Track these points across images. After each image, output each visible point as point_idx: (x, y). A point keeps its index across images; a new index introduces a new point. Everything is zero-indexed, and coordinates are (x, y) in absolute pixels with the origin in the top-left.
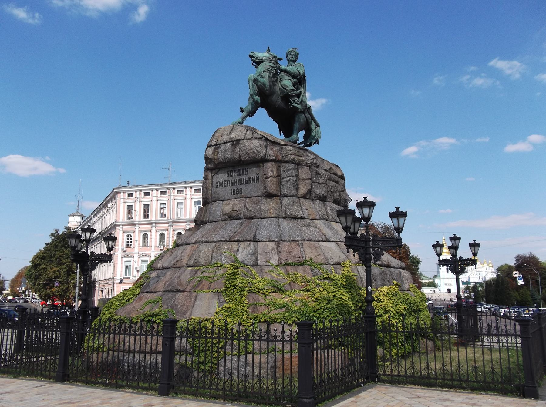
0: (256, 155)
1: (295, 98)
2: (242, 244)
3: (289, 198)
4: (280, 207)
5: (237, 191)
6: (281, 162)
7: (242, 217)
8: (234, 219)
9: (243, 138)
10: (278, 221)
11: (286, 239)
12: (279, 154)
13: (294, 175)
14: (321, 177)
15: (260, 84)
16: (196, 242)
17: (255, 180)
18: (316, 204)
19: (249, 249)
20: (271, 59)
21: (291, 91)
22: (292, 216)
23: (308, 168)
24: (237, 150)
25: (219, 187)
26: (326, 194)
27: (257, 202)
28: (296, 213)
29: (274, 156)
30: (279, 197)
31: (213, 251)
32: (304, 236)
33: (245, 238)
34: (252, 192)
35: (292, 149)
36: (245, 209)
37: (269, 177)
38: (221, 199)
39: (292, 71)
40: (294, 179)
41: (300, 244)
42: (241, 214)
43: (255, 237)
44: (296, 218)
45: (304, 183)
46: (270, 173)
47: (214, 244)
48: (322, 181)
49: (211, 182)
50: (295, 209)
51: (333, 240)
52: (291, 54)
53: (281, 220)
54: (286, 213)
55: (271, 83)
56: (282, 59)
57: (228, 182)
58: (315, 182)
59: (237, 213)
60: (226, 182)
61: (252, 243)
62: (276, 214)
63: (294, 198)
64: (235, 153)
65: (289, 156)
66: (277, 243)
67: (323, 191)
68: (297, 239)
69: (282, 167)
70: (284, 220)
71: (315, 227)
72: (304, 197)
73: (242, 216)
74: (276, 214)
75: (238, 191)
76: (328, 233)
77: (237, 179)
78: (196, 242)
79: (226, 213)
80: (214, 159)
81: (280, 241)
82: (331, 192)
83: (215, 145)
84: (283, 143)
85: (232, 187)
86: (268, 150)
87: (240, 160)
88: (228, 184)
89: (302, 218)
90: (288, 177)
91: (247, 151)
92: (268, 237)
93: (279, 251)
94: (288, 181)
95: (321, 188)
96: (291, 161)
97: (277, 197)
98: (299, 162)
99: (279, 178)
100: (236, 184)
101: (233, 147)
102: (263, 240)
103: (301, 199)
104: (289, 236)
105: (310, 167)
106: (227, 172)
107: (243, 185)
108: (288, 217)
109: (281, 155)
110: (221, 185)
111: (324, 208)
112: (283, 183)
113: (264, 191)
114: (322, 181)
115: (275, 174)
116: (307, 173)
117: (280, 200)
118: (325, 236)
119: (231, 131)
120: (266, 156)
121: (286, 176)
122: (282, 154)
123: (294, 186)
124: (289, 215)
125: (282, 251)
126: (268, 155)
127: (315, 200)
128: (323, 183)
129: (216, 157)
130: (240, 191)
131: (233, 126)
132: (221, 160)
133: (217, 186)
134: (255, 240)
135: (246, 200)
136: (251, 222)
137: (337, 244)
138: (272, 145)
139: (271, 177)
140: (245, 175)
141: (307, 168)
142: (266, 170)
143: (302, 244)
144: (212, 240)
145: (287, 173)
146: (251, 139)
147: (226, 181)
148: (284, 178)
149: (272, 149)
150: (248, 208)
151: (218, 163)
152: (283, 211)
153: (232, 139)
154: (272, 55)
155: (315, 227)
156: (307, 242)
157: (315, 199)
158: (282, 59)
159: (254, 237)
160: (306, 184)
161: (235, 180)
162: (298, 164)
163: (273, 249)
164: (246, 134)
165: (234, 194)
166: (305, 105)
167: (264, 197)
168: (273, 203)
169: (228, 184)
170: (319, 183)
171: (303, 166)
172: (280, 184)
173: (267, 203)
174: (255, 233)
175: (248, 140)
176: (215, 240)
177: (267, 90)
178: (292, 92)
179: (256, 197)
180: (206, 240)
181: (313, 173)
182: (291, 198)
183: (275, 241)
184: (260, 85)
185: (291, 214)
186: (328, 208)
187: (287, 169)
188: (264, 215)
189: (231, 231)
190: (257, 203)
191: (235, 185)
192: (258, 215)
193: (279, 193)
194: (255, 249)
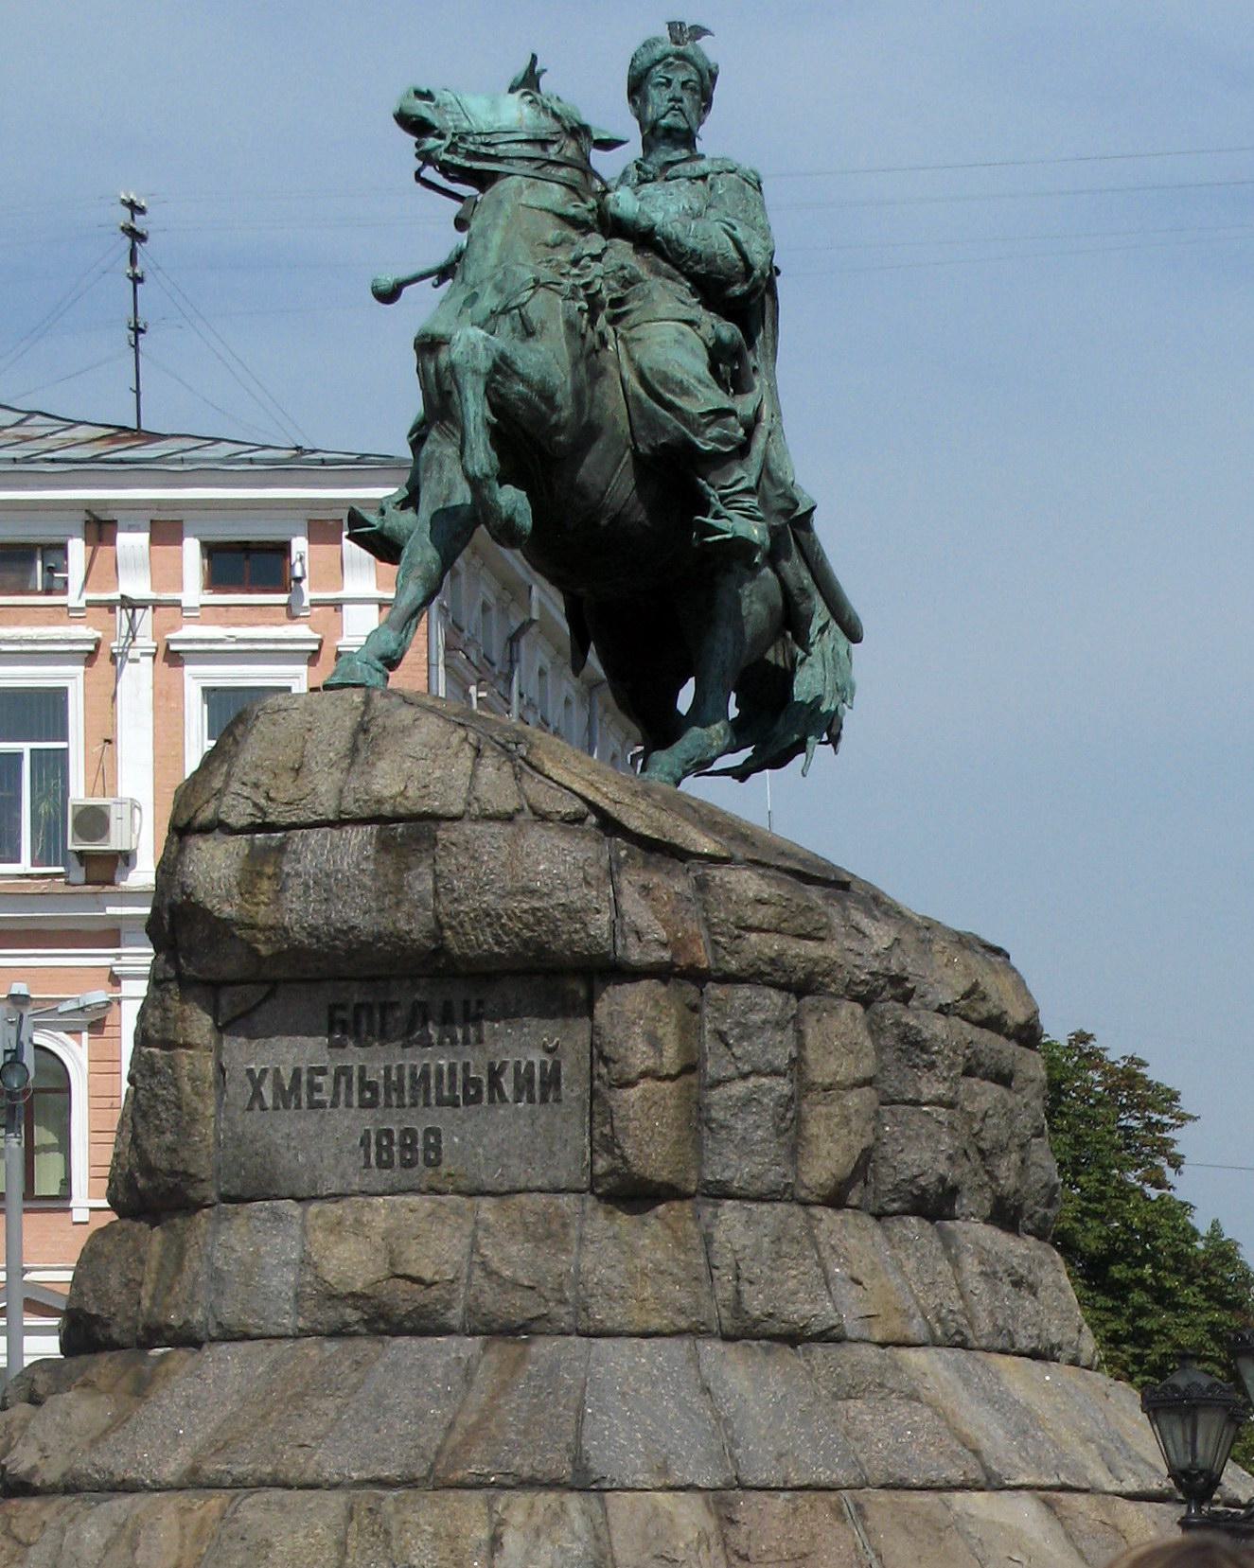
0: (555, 933)
1: (730, 472)
2: (518, 1508)
3: (753, 1206)
4: (704, 1271)
5: (404, 1146)
6: (697, 976)
7: (455, 1323)
8: (397, 1331)
9: (457, 808)
10: (695, 1359)
11: (762, 1477)
12: (693, 927)
13: (782, 1062)
14: (931, 1066)
15: (521, 388)
16: (194, 1482)
17: (531, 1081)
18: (904, 1239)
19: (562, 1533)
20: (553, 149)
21: (708, 425)
22: (776, 1327)
23: (859, 1009)
24: (421, 882)
25: (269, 1102)
26: (952, 1176)
27: (555, 1226)
28: (801, 1310)
29: (664, 945)
30: (688, 1203)
31: (342, 1545)
32: (863, 1457)
33: (524, 1465)
34: (515, 1161)
35: (767, 891)
36: (478, 1273)
37: (633, 1076)
38: (285, 1186)
39: (690, 243)
40: (783, 1086)
41: (848, 1507)
42: (448, 1306)
43: (578, 1458)
44: (794, 1338)
45: (835, 1109)
46: (640, 1057)
47: (336, 1500)
48: (932, 1088)
49: (211, 1065)
50: (792, 1284)
51: (1023, 1480)
52: (669, 83)
53: (711, 1348)
54: (737, 1307)
55: (582, 368)
56: (620, 143)
57: (337, 1082)
58: (894, 1102)
59: (423, 1296)
60: (320, 1079)
61: (574, 1502)
62: (681, 1311)
63: (779, 1206)
64: (406, 907)
65: (754, 937)
66: (719, 1502)
67: (942, 1157)
68: (824, 1476)
69: (707, 1010)
70: (732, 1351)
71: (913, 1397)
72: (836, 1199)
73: (455, 1316)
74: (681, 1311)
75: (411, 1148)
76: (989, 1437)
77: (400, 1068)
78: (194, 1482)
79: (343, 1290)
80: (252, 927)
81: (728, 1487)
82: (981, 1151)
83: (253, 828)
84: (706, 845)
85: (367, 1113)
86: (626, 904)
87: (441, 951)
88: (336, 1094)
89: (832, 1336)
90: (745, 1076)
91: (489, 898)
92: (659, 1461)
93: (736, 1552)
94: (747, 1102)
95: (930, 1136)
96: (761, 974)
97: (676, 1204)
98: (810, 976)
99: (692, 1079)
100: (401, 1098)
101: (388, 860)
102: (628, 1483)
103: (817, 1211)
104: (780, 1455)
105: (866, 1001)
106: (333, 1008)
107: (447, 1111)
108: (744, 1331)
109: (704, 932)
110: (286, 1096)
111: (943, 1266)
112: (717, 1114)
113: (602, 1164)
114: (932, 1088)
115: (670, 1058)
116: (852, 1049)
117: (697, 1218)
118: (976, 1453)
119: (355, 735)
120: (619, 942)
121: (731, 1071)
122: (710, 926)
123: (780, 1133)
124: (757, 1322)
125: (752, 1554)
126: (632, 939)
127: (895, 1213)
128: (939, 1102)
129: (263, 915)
130: (428, 1147)
131: (367, 702)
132: (299, 935)
133: (257, 1095)
134: (586, 1483)
135: (475, 1210)
136: (523, 1358)
137: (1049, 1505)
138: (646, 866)
139: (644, 1075)
140: (459, 1047)
141: (852, 1014)
142: (619, 1033)
143: (858, 1506)
144: (309, 1476)
145: (738, 1051)
146: (508, 818)
147: (322, 1071)
148: (718, 1083)
149: (646, 890)
150: (495, 1264)
151: (278, 955)
152: (720, 1294)
153: (379, 802)
154: (556, 116)
155: (913, 1397)
156: (883, 1497)
157: (896, 1206)
158: (620, 143)
159: (573, 1461)
160: (846, 1120)
161: (388, 1069)
162: (802, 986)
163: (703, 1539)
164: (473, 776)
165: (382, 1165)
166: (781, 504)
167: (599, 1197)
168: (655, 1237)
169: (336, 1094)
170: (916, 1103)
171: (826, 1002)
172: (697, 1122)
173: (615, 1237)
174: (578, 1435)
175: (496, 827)
176: (330, 1472)
177: (558, 428)
178: (714, 431)
179: (543, 1198)
180: (269, 1469)
181: (888, 1040)
182: (765, 1207)
183: (700, 1489)
184: (523, 398)
185: (770, 1315)
186: (971, 1265)
187: (738, 1024)
188: (602, 1314)
189: (421, 1415)
190: (550, 1234)
191: (388, 1105)
192: (563, 1310)
193: (693, 1175)
194: (598, 1538)
